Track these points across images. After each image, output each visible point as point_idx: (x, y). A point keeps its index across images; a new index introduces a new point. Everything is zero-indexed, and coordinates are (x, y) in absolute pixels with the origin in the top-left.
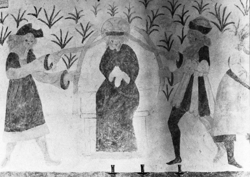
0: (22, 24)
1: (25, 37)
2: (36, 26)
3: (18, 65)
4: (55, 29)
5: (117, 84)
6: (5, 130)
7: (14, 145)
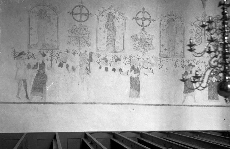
0: (190, 63)
1: (190, 67)
2: (193, 64)
3: (187, 75)
4: (198, 65)
5: (214, 82)
6: (184, 93)
7: (186, 97)
